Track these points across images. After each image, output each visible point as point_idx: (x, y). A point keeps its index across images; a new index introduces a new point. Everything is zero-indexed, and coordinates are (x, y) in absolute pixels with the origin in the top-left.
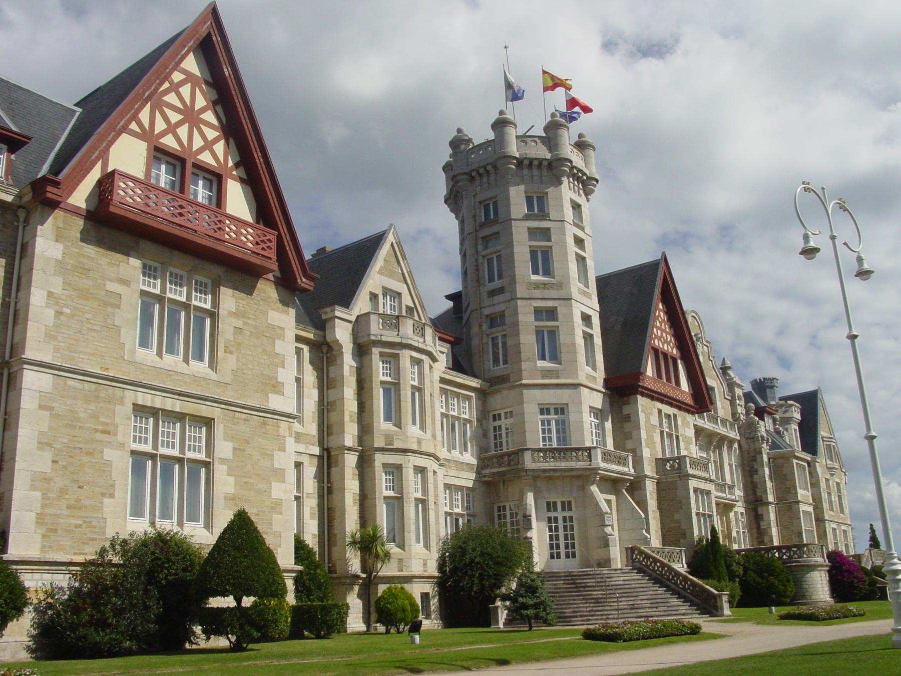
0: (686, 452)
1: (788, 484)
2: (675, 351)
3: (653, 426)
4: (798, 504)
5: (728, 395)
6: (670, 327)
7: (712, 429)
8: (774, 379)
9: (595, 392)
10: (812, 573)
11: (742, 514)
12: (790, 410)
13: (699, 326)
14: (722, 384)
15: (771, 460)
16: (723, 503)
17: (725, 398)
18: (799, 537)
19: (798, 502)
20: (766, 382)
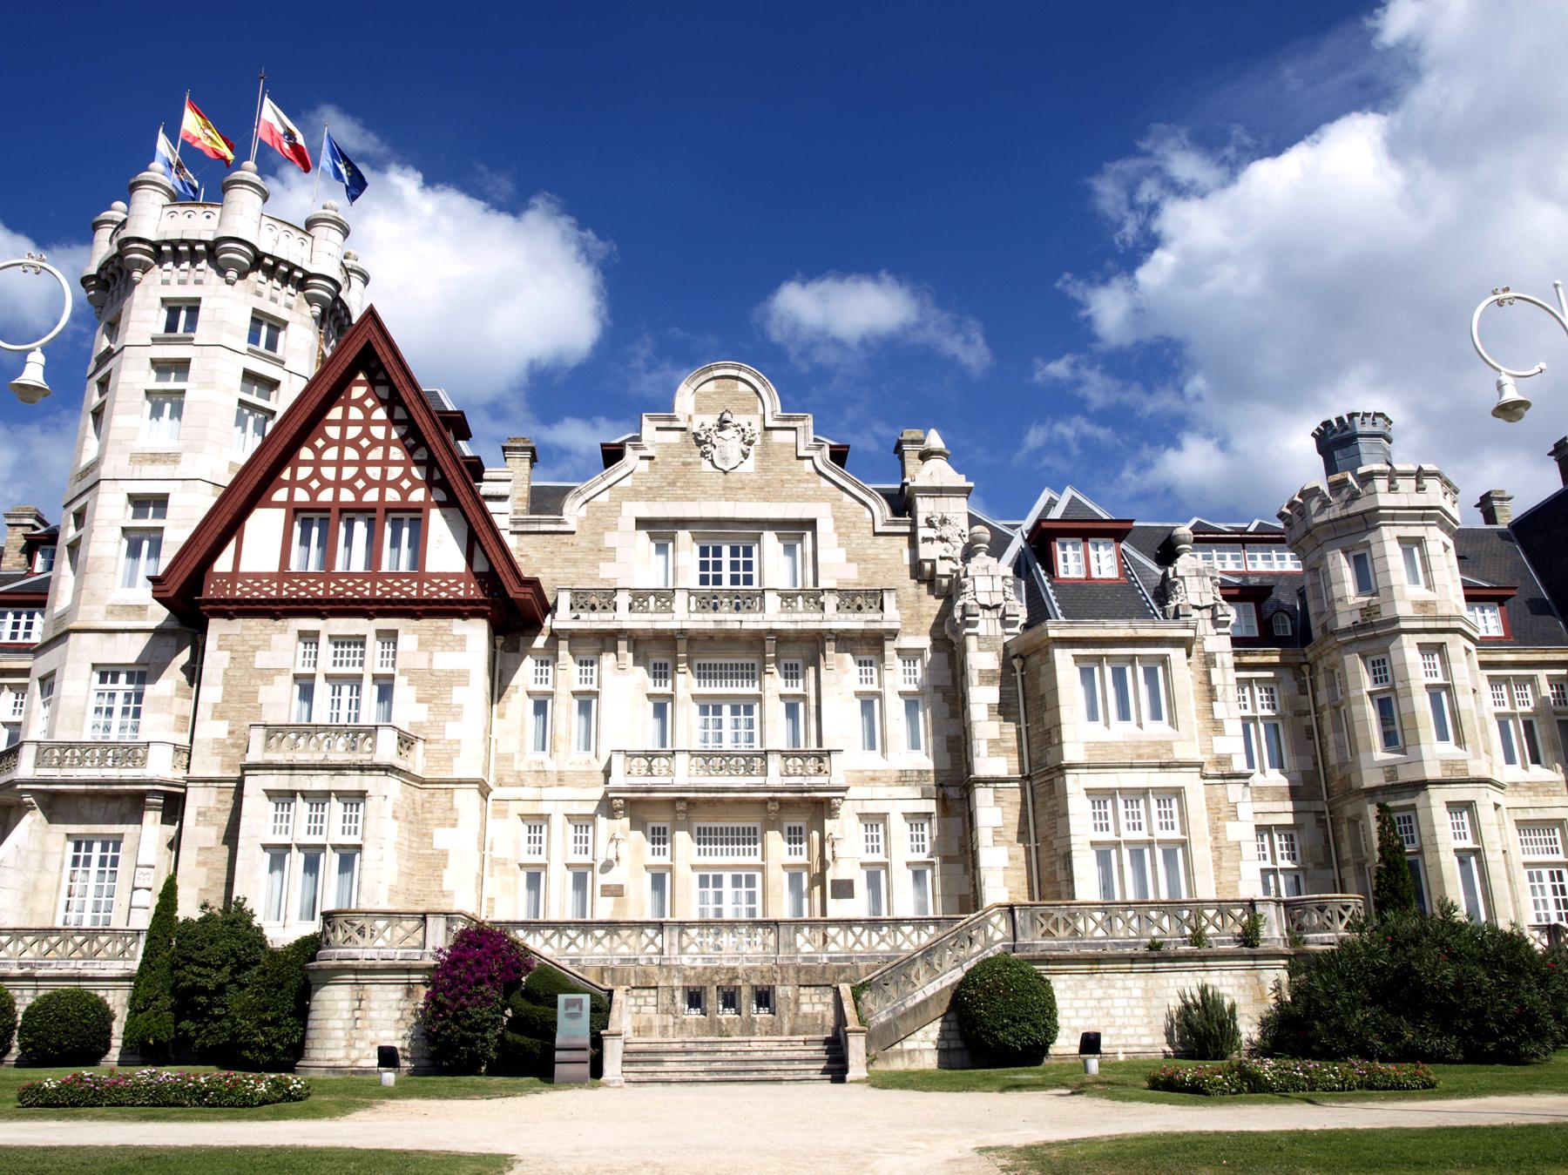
0: (425, 706)
1: (1047, 716)
2: (418, 495)
3: (267, 675)
4: (1063, 775)
5: (896, 523)
6: (410, 451)
7: (711, 626)
8: (1351, 416)
9: (119, 635)
10: (326, 988)
11: (914, 819)
12: (1369, 487)
13: (757, 392)
14: (864, 503)
15: (1015, 662)
16: (770, 799)
17: (876, 534)
18: (1065, 869)
19: (1061, 769)
20: (1329, 432)
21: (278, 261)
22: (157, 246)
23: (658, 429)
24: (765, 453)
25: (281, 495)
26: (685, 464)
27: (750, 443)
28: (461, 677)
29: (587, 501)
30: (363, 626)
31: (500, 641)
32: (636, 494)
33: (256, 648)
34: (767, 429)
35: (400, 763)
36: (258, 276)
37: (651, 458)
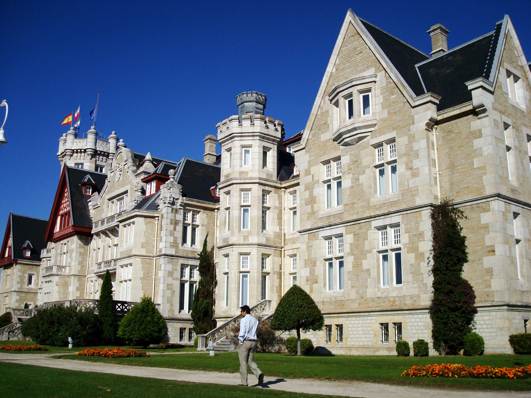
21: (77, 150)
22: (61, 155)
23: (111, 173)
24: (123, 173)
25: (60, 213)
26: (114, 181)
27: (121, 171)
28: (72, 251)
29: (102, 197)
30: (65, 241)
31: (90, 238)
32: (109, 193)
33: (58, 249)
34: (124, 165)
35: (59, 273)
36: (75, 155)
37: (110, 181)
